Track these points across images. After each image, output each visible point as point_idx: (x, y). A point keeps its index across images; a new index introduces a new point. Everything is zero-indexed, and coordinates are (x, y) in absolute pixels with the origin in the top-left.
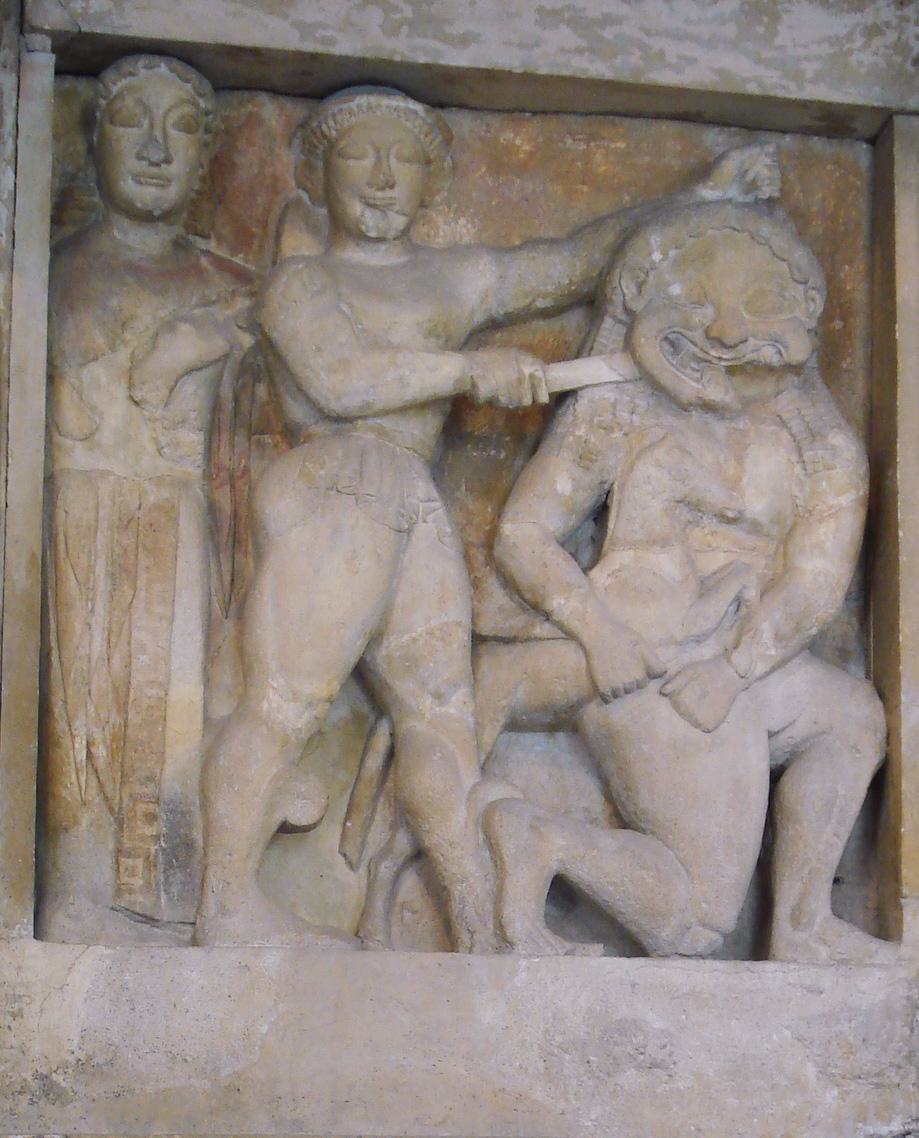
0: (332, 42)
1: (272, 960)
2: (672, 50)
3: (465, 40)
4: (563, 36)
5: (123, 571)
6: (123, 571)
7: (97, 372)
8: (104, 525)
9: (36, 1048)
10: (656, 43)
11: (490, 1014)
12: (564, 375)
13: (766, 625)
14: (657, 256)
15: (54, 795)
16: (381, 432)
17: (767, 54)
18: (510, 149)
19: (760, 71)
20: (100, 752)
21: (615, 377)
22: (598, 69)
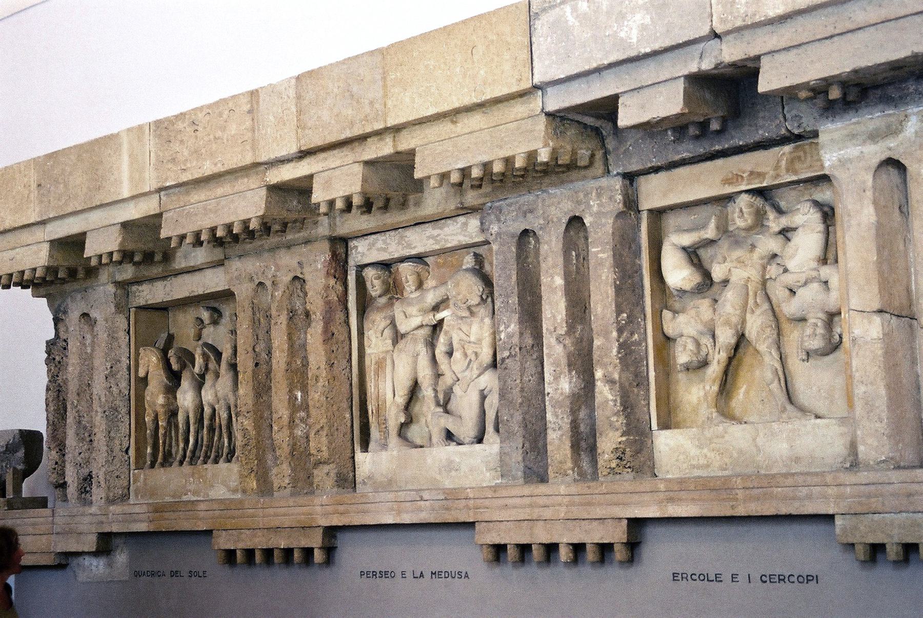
0: (394, 255)
1: (395, 453)
2: (449, 238)
3: (415, 247)
4: (431, 241)
5: (377, 374)
6: (377, 374)
7: (371, 332)
8: (373, 364)
9: (362, 474)
10: (446, 238)
11: (429, 461)
12: (439, 316)
13: (475, 366)
14: (450, 287)
15: (783, 335)
16: (413, 334)
17: (466, 234)
18: (440, 263)
19: (466, 238)
20: (374, 411)
21: (449, 314)
22: (437, 247)
